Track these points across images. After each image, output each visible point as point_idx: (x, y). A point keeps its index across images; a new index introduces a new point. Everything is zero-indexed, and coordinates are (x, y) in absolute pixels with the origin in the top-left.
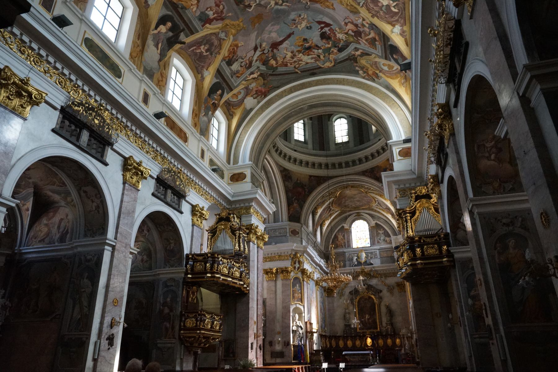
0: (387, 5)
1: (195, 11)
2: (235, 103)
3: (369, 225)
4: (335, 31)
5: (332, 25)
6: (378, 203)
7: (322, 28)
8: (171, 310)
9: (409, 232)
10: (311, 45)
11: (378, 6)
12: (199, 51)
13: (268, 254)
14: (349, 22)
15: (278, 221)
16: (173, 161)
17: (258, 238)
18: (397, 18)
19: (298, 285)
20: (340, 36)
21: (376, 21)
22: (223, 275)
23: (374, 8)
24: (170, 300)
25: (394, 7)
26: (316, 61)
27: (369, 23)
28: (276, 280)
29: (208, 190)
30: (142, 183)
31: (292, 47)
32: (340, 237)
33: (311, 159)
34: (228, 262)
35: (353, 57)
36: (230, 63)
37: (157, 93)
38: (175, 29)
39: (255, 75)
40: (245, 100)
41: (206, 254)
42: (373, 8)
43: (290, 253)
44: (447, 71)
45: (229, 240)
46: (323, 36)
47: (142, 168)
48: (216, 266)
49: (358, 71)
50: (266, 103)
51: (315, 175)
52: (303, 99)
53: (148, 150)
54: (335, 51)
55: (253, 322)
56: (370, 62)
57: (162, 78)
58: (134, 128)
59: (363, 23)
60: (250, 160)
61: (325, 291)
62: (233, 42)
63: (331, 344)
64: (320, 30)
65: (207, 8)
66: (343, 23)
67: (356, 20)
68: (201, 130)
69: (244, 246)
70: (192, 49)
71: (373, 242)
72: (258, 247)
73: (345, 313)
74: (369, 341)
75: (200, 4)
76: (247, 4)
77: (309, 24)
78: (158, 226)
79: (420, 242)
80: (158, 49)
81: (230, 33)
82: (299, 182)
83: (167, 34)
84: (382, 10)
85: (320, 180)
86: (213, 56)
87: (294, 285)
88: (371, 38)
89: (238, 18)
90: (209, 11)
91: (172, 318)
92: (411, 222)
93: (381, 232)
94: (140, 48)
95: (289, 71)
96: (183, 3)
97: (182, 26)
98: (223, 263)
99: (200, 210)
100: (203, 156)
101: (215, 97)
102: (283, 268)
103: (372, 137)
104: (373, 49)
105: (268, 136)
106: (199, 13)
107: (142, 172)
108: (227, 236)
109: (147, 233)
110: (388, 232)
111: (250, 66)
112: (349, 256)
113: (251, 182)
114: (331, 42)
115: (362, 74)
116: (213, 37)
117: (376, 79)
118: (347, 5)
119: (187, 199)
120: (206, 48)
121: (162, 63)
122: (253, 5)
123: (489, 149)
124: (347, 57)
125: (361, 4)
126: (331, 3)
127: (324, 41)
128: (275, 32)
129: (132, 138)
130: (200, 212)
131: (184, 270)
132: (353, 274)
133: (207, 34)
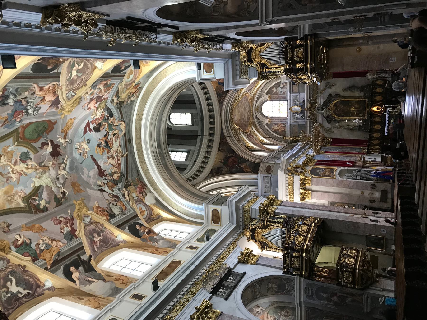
0: (77, 72)
1: (63, 243)
2: (148, 213)
3: (267, 101)
4: (94, 119)
5: (89, 121)
6: (248, 91)
7: (90, 130)
8: (334, 294)
9: (280, 71)
10: (104, 141)
11: (77, 79)
12: (98, 242)
14: (88, 106)
15: (257, 183)
16: (197, 277)
17: (272, 205)
18: (89, 64)
19: (318, 171)
20: (99, 114)
21: (90, 83)
22: (305, 241)
23: (78, 83)
24: (325, 294)
25: (79, 66)
26: (118, 137)
27: (90, 88)
28: (312, 191)
29: (225, 246)
30: (215, 309)
31: (104, 157)
32: (276, 127)
33: (204, 148)
34: (293, 235)
35: (118, 104)
36: (112, 215)
37: (134, 286)
39: (126, 193)
40: (147, 203)
41: (284, 255)
42: (78, 84)
43: (287, 176)
44: (147, 33)
45: (271, 232)
46: (97, 129)
47: (202, 308)
48: (296, 247)
49: (131, 101)
50: (151, 185)
51: (218, 147)
52: (151, 152)
53: (185, 300)
54: (112, 120)
55: (351, 218)
56: (125, 91)
57: (120, 280)
58: (165, 311)
59: (90, 94)
60: (201, 204)
61: (325, 146)
62: (94, 210)
64: (91, 132)
65: (61, 232)
66: (88, 111)
67: (87, 99)
68: (170, 247)
69: (279, 218)
70: (96, 249)
71: (284, 99)
72: (280, 205)
73: (347, 129)
74: (375, 109)
75: (56, 238)
76: (61, 196)
77: (85, 141)
78: (255, 297)
79: (290, 64)
80: (94, 281)
81: (86, 213)
82: (223, 161)
83: (81, 271)
84: (81, 77)
85: (223, 142)
86: (104, 230)
87: (317, 175)
88: (104, 88)
89: (73, 204)
90: (64, 231)
91: (343, 295)
92: (271, 68)
93: (275, 90)
94: (91, 298)
95: (125, 162)
97: (75, 257)
98: (294, 240)
99: (243, 256)
100: (195, 248)
101: (142, 231)
103: (190, 93)
104: (113, 86)
105: (181, 186)
106: (64, 240)
107: (205, 308)
108: (269, 232)
109: (260, 309)
111: (117, 197)
113: (221, 205)
114: (104, 123)
115: (134, 98)
116: (88, 229)
117: (140, 86)
118: (73, 106)
119: (232, 267)
120: (97, 236)
121: (107, 279)
122: (63, 190)
123: (218, 3)
124: (118, 109)
125: (73, 94)
126: (69, 120)
127: (101, 129)
128: (89, 172)
129: (173, 314)
130: (245, 256)
131: (298, 277)
132: (311, 118)
133: (85, 234)
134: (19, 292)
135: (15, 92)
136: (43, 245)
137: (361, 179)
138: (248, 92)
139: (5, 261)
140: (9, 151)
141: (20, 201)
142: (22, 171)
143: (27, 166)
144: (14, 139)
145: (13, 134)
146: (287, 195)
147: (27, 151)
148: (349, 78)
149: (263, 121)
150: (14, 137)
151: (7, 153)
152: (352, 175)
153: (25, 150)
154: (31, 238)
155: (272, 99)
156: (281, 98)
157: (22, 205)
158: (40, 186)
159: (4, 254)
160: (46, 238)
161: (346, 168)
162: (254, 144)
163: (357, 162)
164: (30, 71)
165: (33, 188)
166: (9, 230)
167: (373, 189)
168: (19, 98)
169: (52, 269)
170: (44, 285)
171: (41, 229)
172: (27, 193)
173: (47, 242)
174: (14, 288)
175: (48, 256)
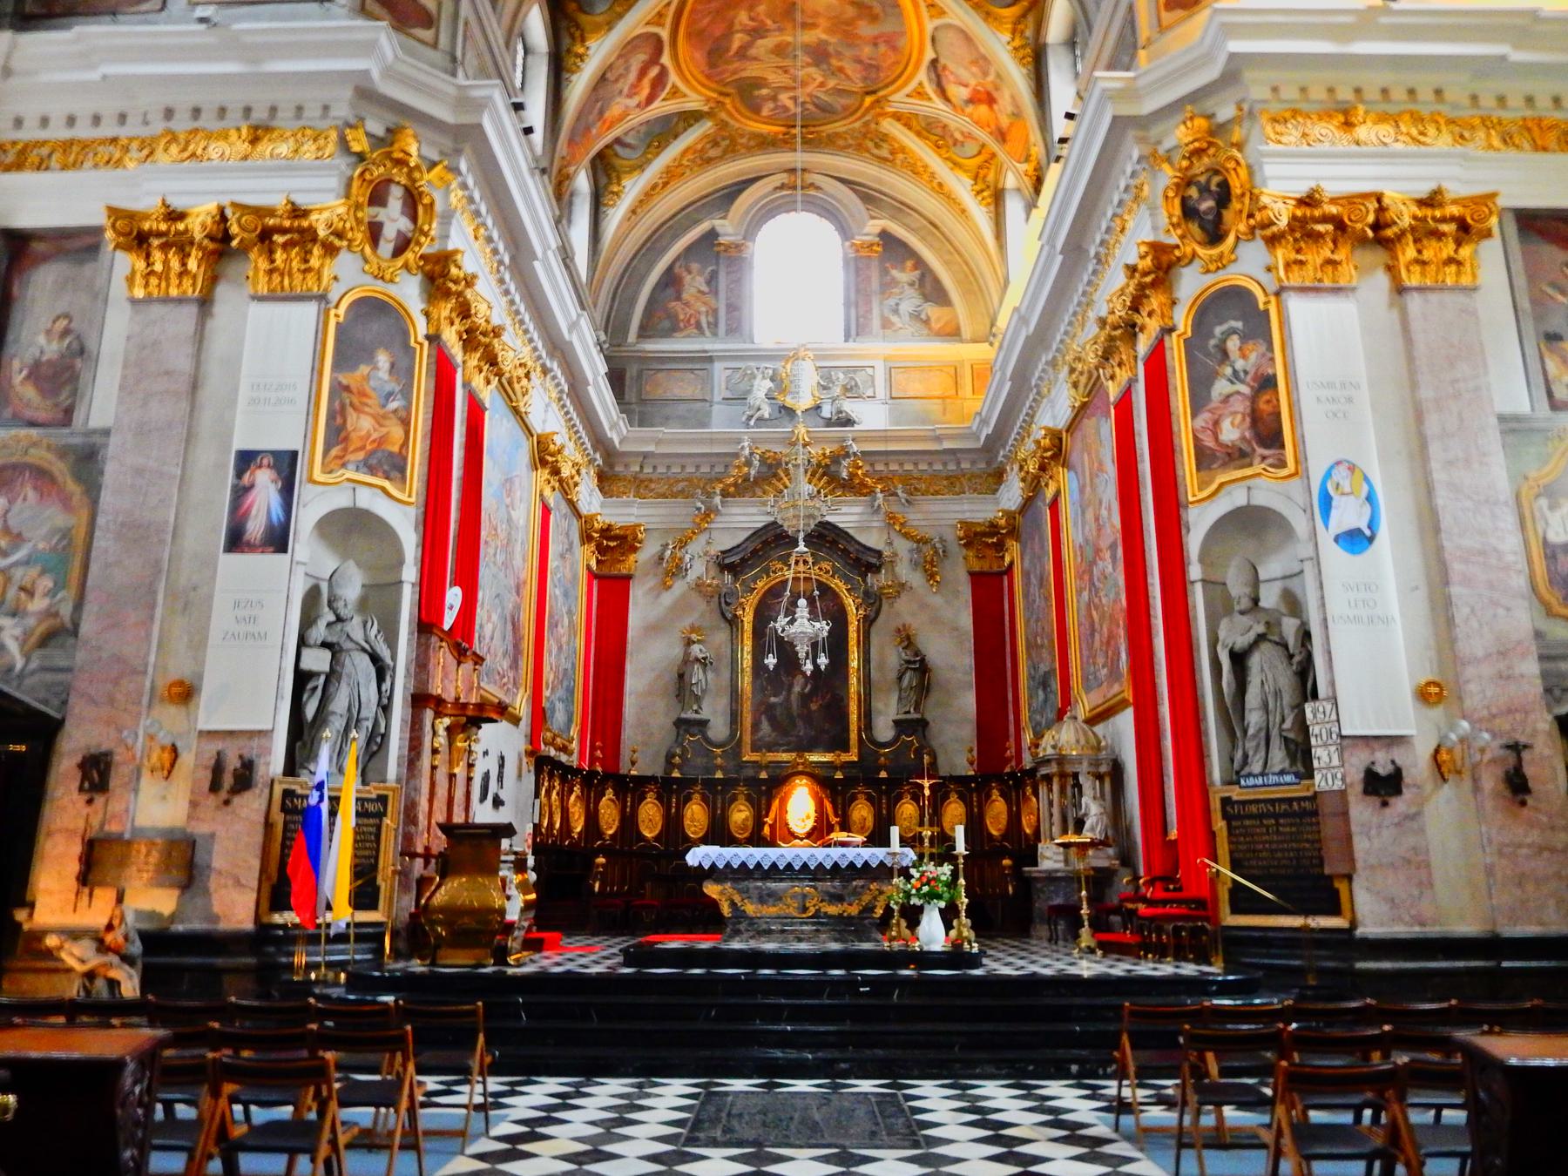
6: (934, 62)
13: (169, 113)
19: (383, 359)
28: (205, 302)
32: (694, 283)
43: (342, 111)
61: (586, 538)
63: (592, 818)
71: (855, 329)
73: (687, 661)
87: (350, 351)
93: (904, 276)
102: (271, 212)
110: (937, 281)
112: (728, 379)
132: (748, 463)
137: (302, 678)
138: (929, 54)
146: (169, 113)
148: (968, 661)
149: (731, 214)
152: (343, 612)
155: (857, 264)
156: (861, 313)
161: (410, 574)
162: (602, 80)
163: (468, 666)
167: (208, 775)
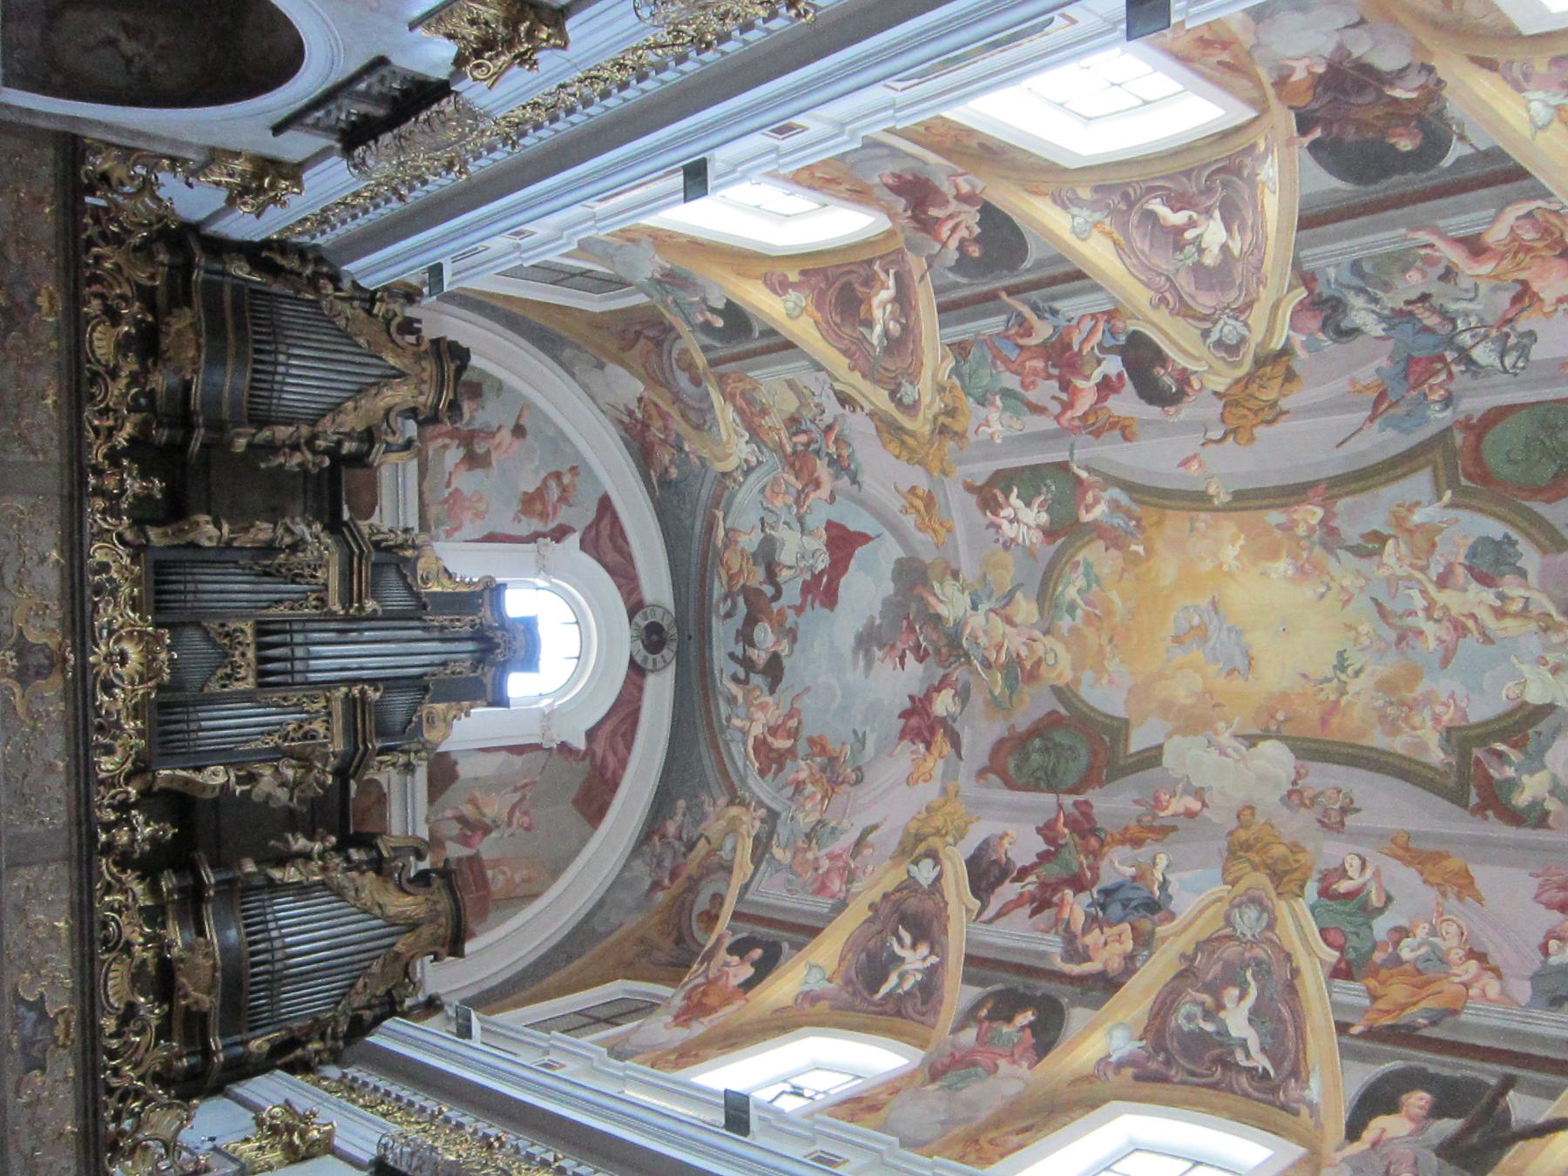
1: (1503, 992)
38: (1448, 1099)
75: (1495, 959)
90: (1561, 949)
96: (1422, 1005)
97: (1490, 1074)
106: (1527, 985)
134: (1244, 1044)
135: (1357, 282)
136: (1420, 946)
139: (1265, 915)
140: (1418, 526)
141: (1433, 739)
142: (1473, 616)
143: (1498, 603)
144: (1436, 476)
145: (1430, 457)
147: (1507, 536)
150: (1435, 469)
151: (1410, 532)
153: (1495, 529)
154: (1393, 893)
157: (1436, 756)
158: (1547, 709)
159: (1273, 894)
160: (1453, 929)
164: (1335, 183)
165: (1511, 705)
166: (1342, 823)
168: (1394, 300)
169: (1361, 1043)
170: (1305, 1085)
171: (1464, 885)
172: (1473, 718)
173: (1444, 946)
174: (1237, 1021)
175: (1398, 991)
